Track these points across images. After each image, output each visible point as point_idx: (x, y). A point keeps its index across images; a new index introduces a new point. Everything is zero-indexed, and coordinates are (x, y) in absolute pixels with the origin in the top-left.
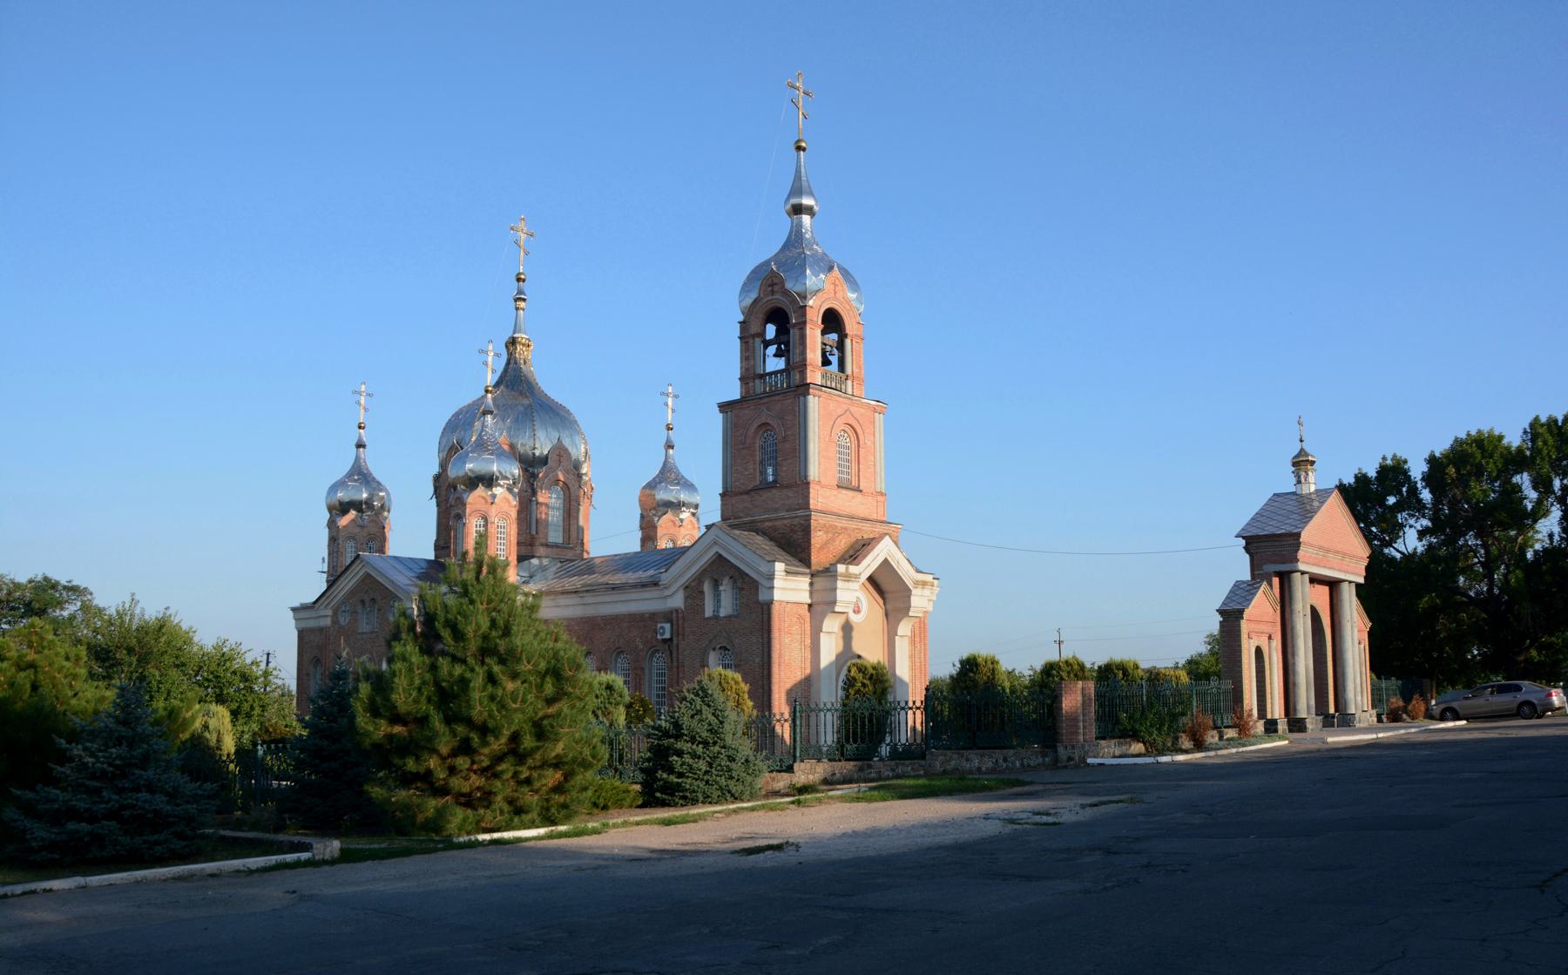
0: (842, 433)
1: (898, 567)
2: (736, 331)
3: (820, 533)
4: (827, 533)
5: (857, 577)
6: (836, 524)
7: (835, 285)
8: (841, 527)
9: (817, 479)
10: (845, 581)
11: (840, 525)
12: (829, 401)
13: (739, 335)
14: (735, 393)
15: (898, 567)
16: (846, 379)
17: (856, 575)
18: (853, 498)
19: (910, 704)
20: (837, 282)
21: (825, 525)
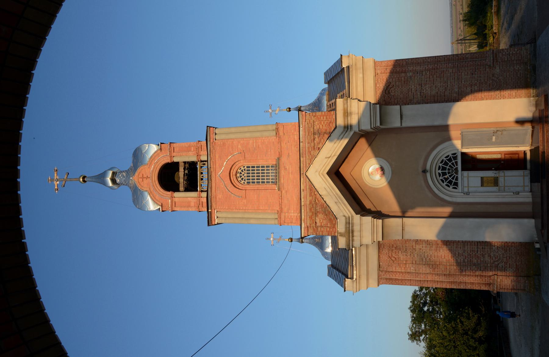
0: (239, 179)
1: (334, 156)
3: (318, 221)
4: (316, 214)
5: (349, 223)
6: (308, 203)
7: (143, 178)
8: (310, 195)
9: (276, 216)
10: (353, 236)
11: (308, 197)
12: (218, 199)
15: (334, 156)
16: (202, 161)
17: (346, 223)
18: (285, 169)
20: (141, 176)
21: (311, 218)
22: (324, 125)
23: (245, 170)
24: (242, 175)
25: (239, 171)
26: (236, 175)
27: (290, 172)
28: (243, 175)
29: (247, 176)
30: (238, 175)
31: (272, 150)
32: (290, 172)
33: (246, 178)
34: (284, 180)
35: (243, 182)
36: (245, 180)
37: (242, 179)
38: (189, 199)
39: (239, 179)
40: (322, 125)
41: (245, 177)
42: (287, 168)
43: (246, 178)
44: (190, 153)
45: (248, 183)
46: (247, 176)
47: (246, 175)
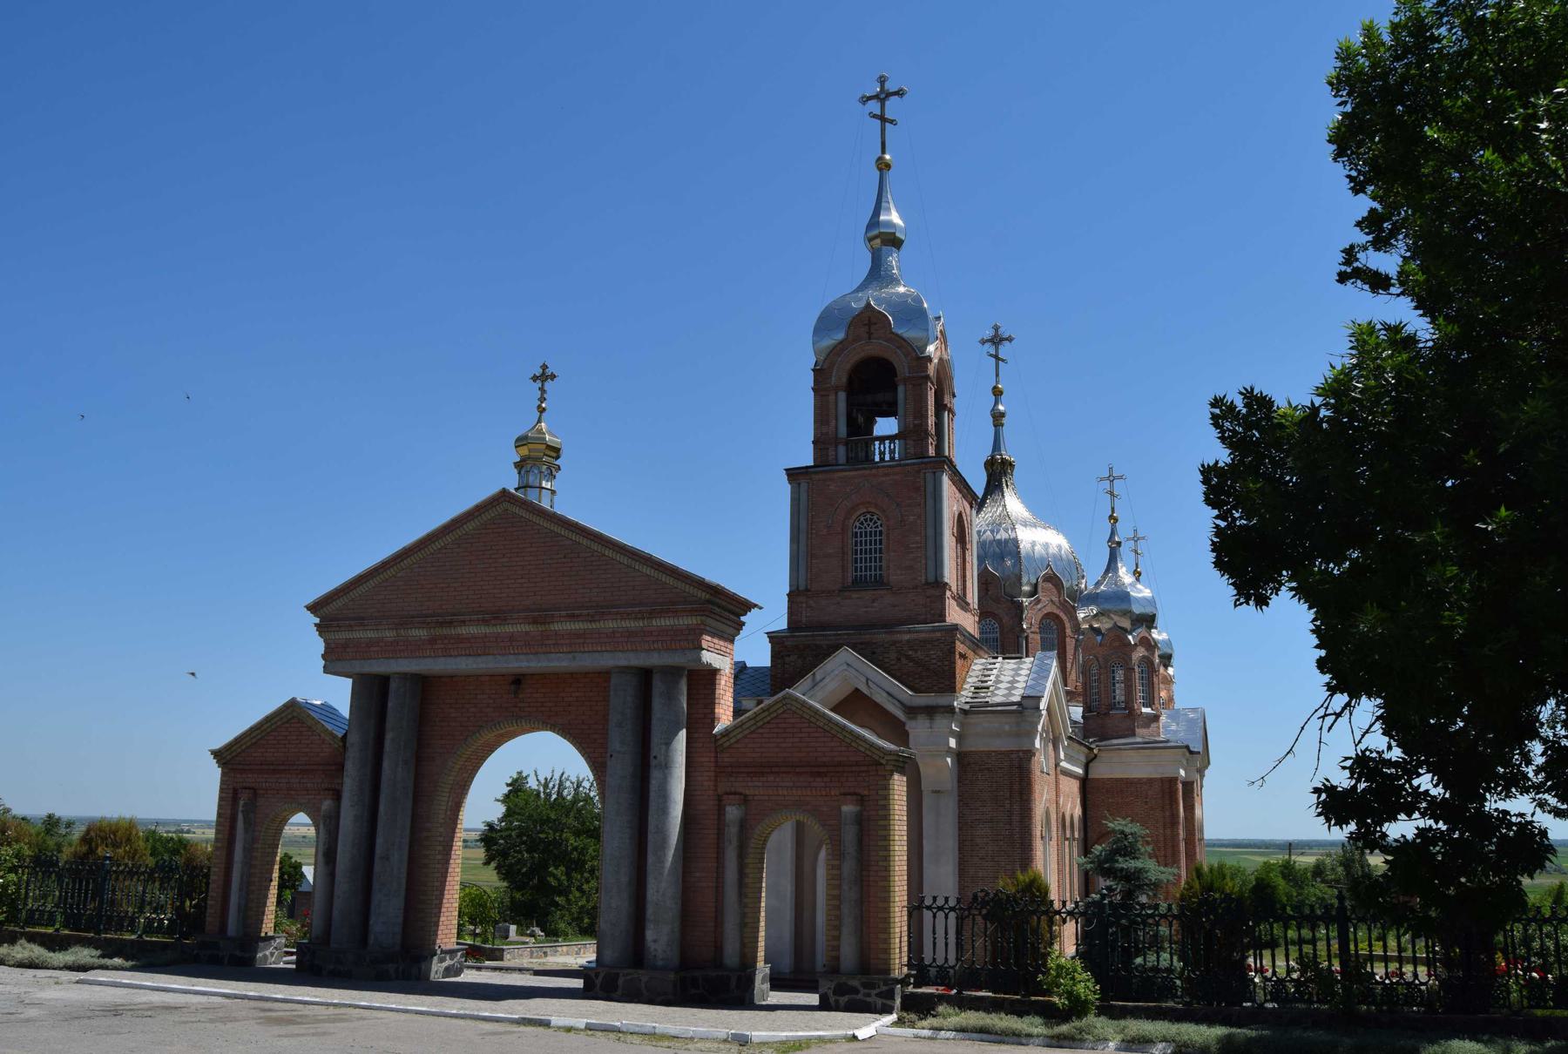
2: (809, 380)
13: (812, 384)
14: (806, 458)
18: (873, 601)
19: (928, 902)
22: (936, 666)
23: (877, 527)
24: (869, 522)
25: (875, 517)
26: (869, 512)
27: (869, 609)
28: (869, 525)
29: (866, 532)
30: (868, 516)
31: (903, 577)
32: (869, 609)
33: (863, 530)
34: (858, 598)
35: (858, 524)
36: (860, 528)
37: (862, 523)
38: (833, 423)
39: (862, 519)
40: (936, 664)
41: (865, 528)
42: (875, 604)
43: (863, 530)
44: (910, 419)
45: (856, 533)
46: (866, 532)
47: (869, 529)
